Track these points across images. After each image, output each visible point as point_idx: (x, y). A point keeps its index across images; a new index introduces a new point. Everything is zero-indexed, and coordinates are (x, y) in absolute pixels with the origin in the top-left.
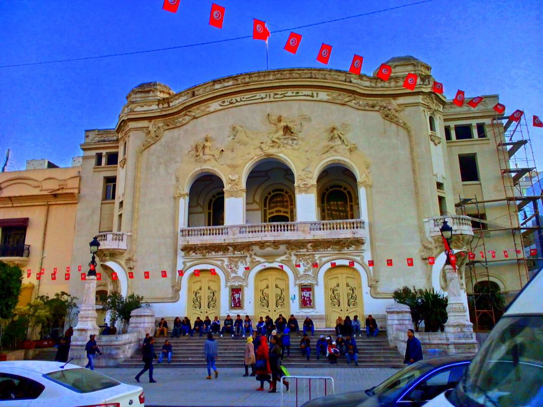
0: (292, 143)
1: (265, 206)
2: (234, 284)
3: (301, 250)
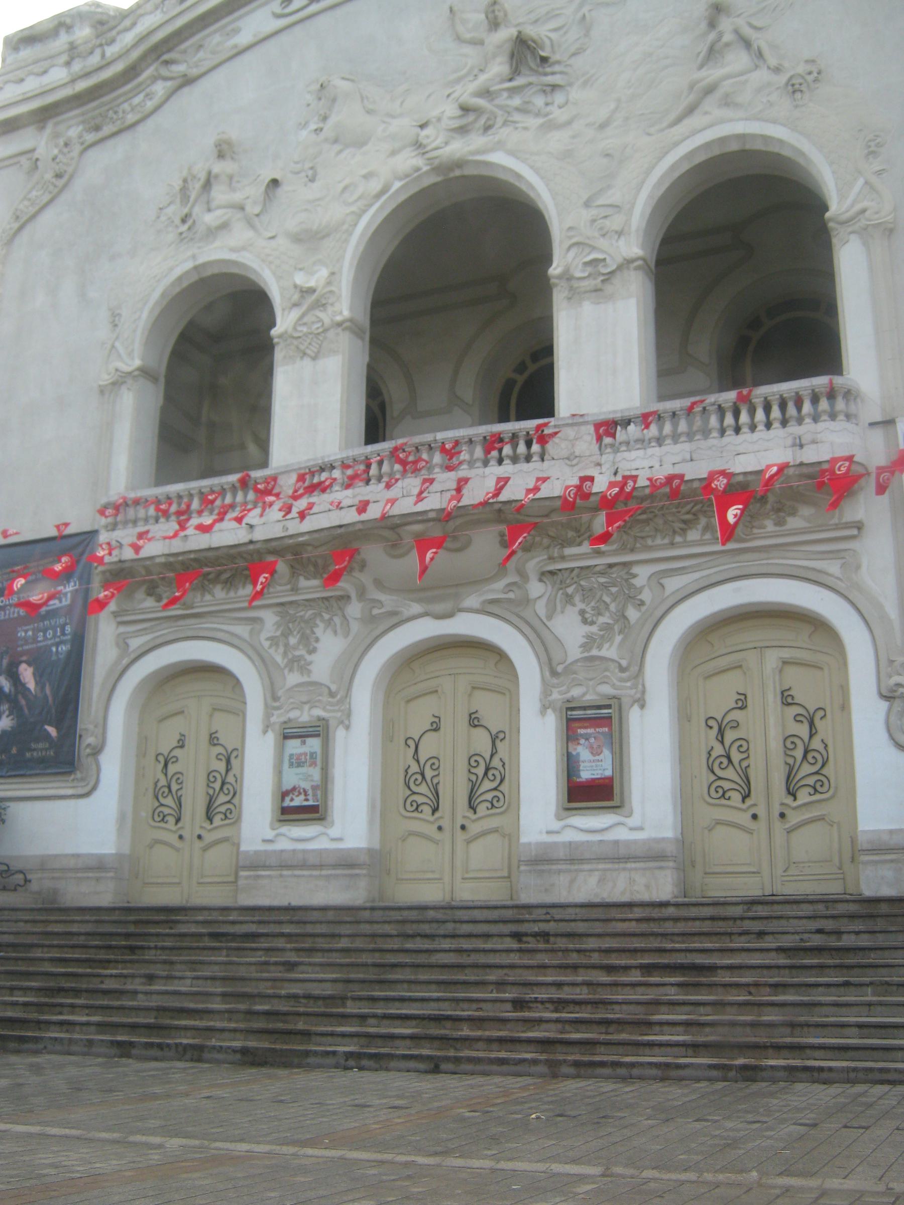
2: (293, 715)
3: (568, 551)
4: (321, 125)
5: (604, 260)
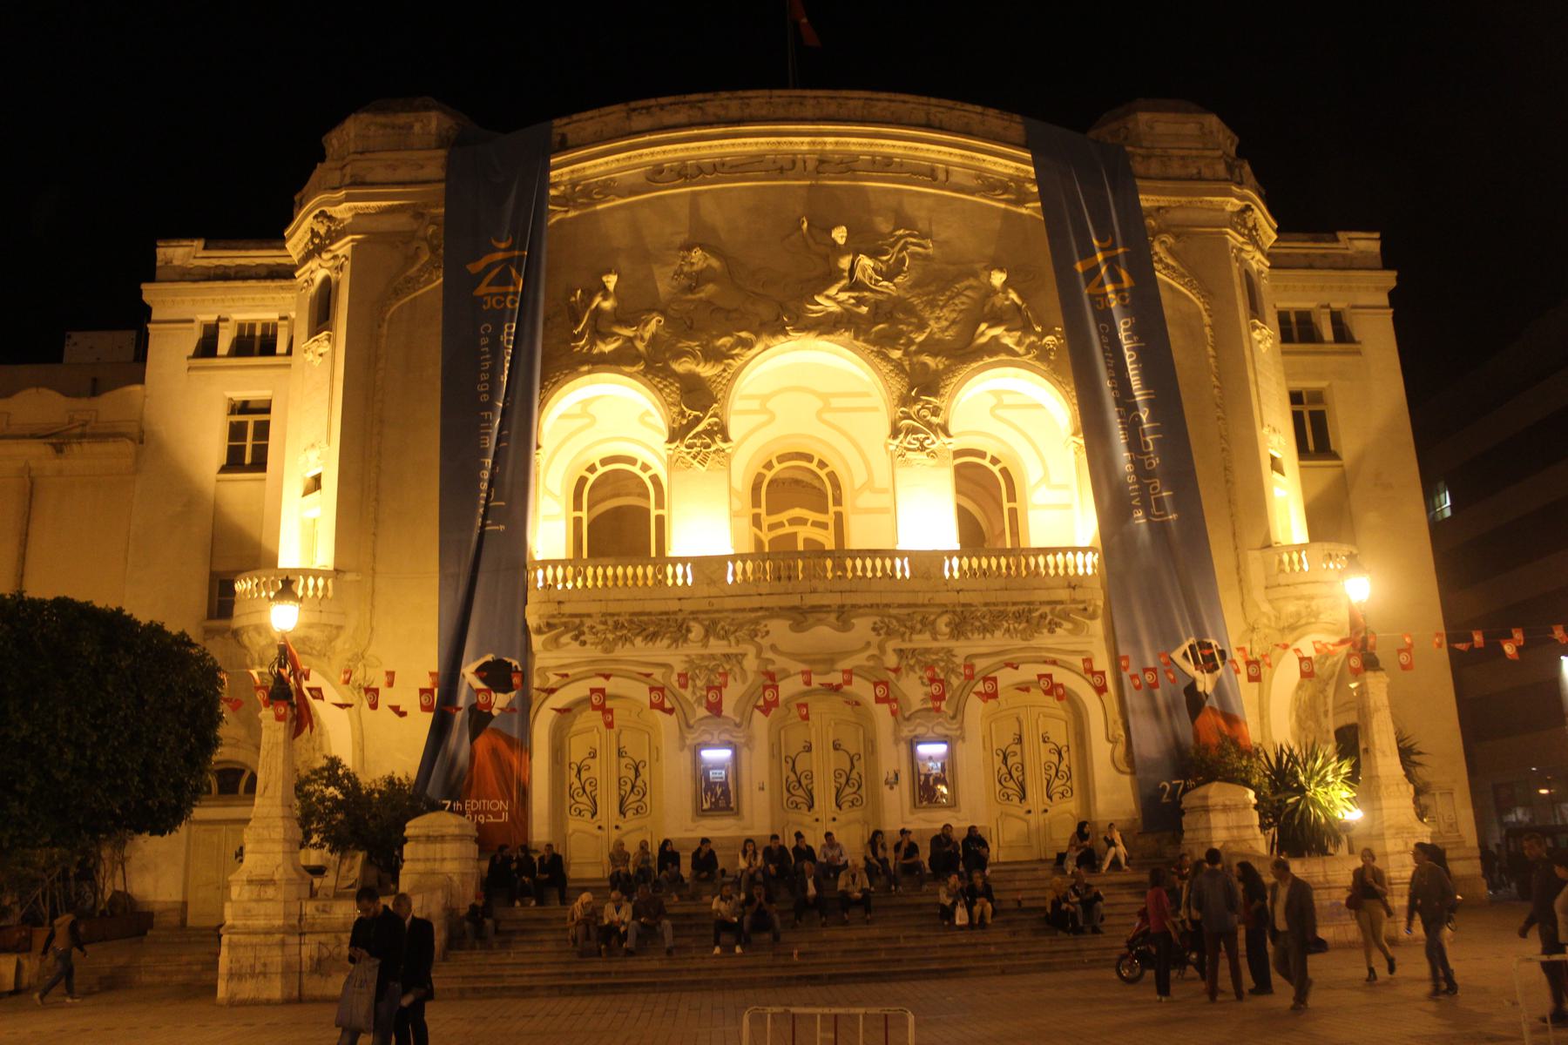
1: (756, 502)
3: (915, 637)
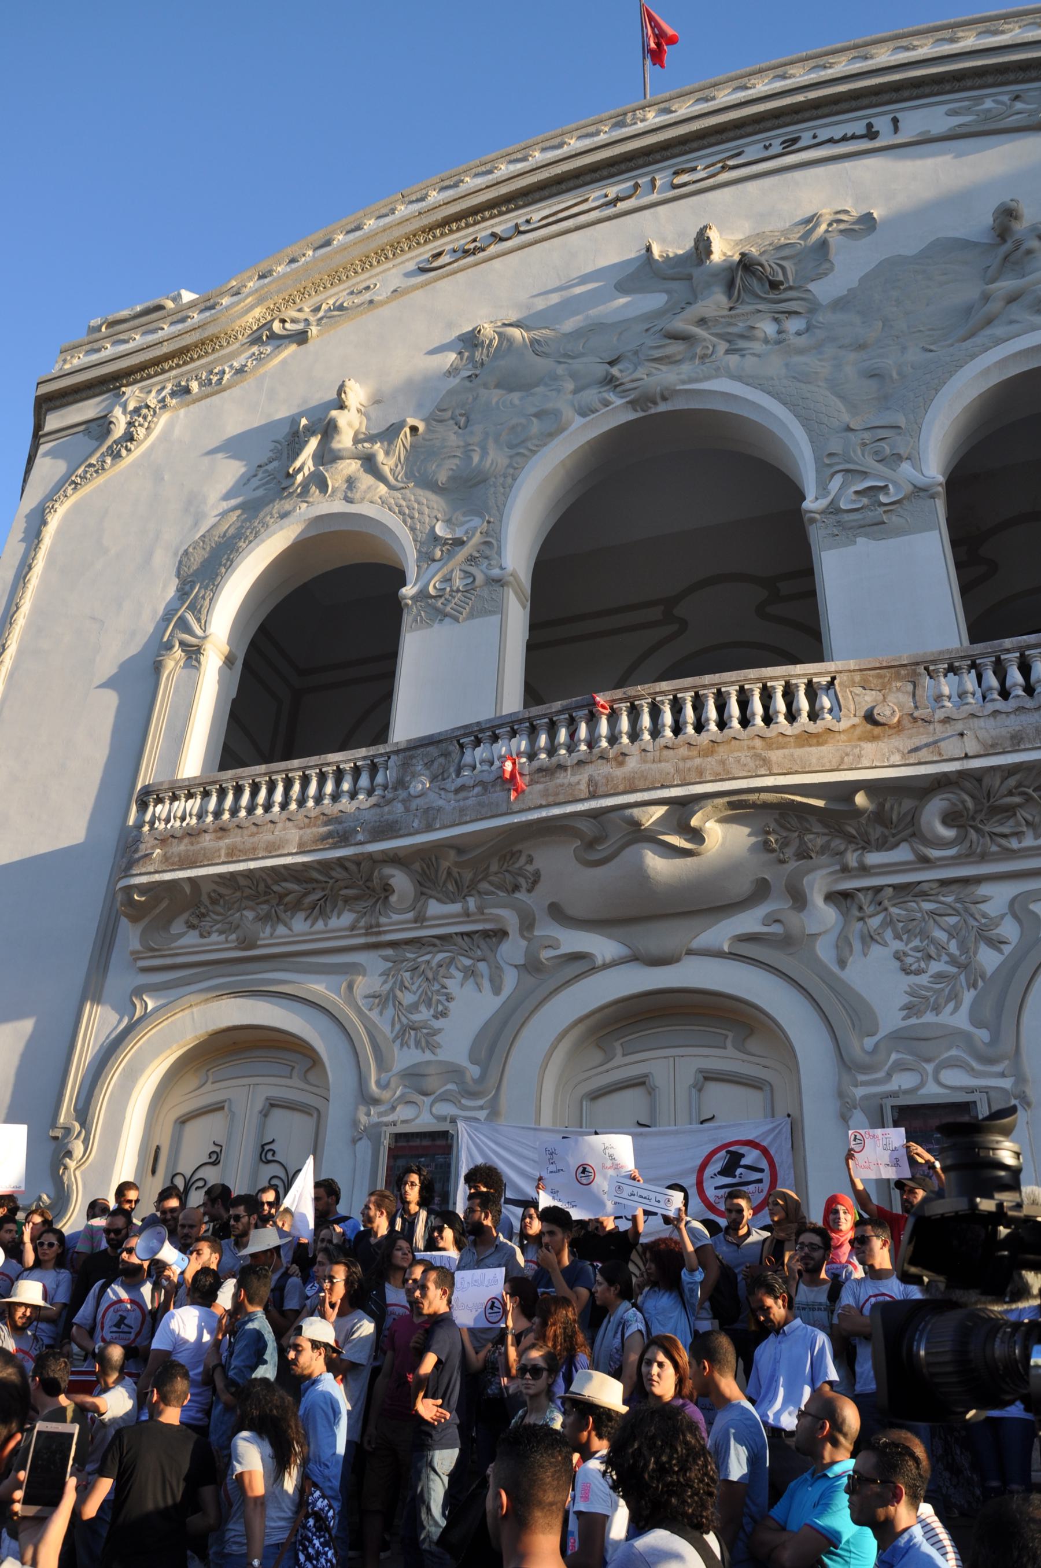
0: (779, 332)
3: (873, 858)
4: (477, 372)
5: (887, 486)
